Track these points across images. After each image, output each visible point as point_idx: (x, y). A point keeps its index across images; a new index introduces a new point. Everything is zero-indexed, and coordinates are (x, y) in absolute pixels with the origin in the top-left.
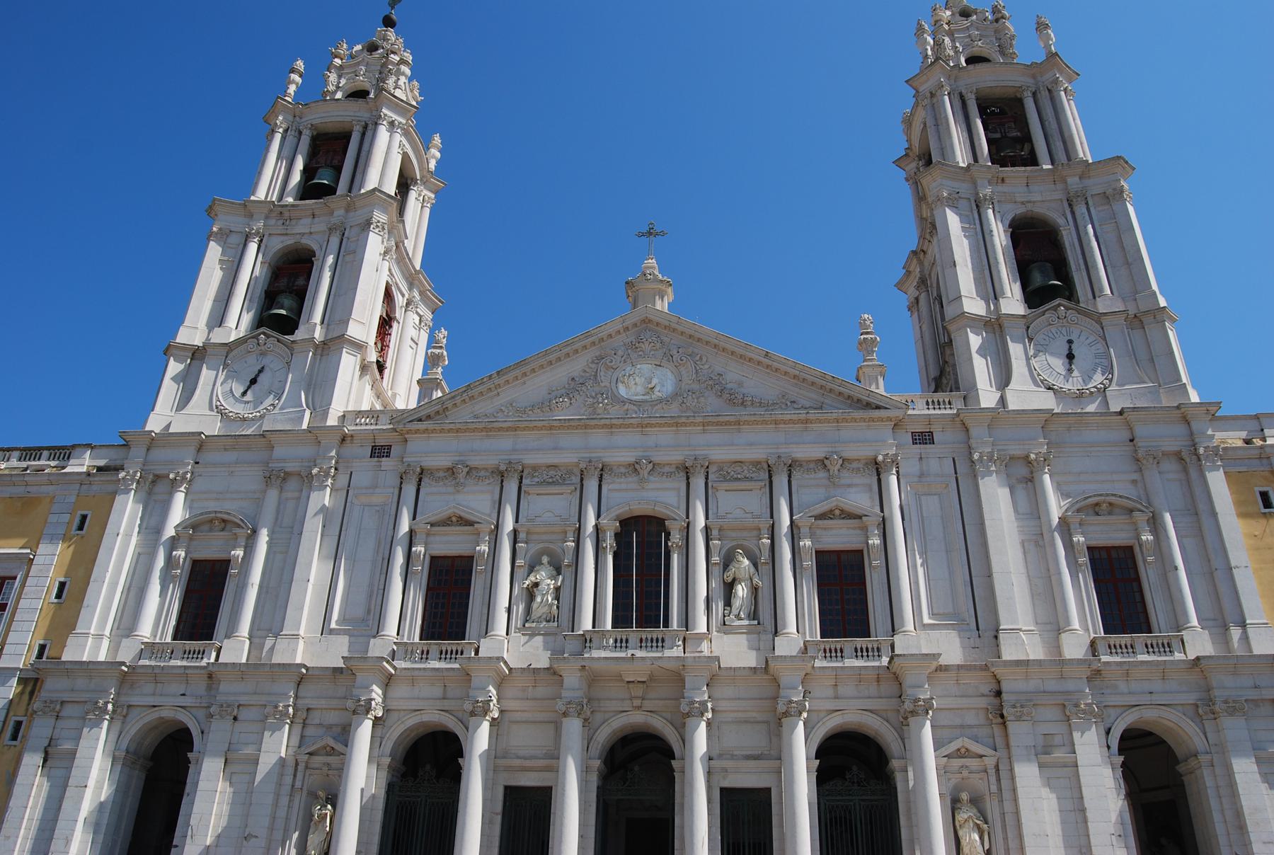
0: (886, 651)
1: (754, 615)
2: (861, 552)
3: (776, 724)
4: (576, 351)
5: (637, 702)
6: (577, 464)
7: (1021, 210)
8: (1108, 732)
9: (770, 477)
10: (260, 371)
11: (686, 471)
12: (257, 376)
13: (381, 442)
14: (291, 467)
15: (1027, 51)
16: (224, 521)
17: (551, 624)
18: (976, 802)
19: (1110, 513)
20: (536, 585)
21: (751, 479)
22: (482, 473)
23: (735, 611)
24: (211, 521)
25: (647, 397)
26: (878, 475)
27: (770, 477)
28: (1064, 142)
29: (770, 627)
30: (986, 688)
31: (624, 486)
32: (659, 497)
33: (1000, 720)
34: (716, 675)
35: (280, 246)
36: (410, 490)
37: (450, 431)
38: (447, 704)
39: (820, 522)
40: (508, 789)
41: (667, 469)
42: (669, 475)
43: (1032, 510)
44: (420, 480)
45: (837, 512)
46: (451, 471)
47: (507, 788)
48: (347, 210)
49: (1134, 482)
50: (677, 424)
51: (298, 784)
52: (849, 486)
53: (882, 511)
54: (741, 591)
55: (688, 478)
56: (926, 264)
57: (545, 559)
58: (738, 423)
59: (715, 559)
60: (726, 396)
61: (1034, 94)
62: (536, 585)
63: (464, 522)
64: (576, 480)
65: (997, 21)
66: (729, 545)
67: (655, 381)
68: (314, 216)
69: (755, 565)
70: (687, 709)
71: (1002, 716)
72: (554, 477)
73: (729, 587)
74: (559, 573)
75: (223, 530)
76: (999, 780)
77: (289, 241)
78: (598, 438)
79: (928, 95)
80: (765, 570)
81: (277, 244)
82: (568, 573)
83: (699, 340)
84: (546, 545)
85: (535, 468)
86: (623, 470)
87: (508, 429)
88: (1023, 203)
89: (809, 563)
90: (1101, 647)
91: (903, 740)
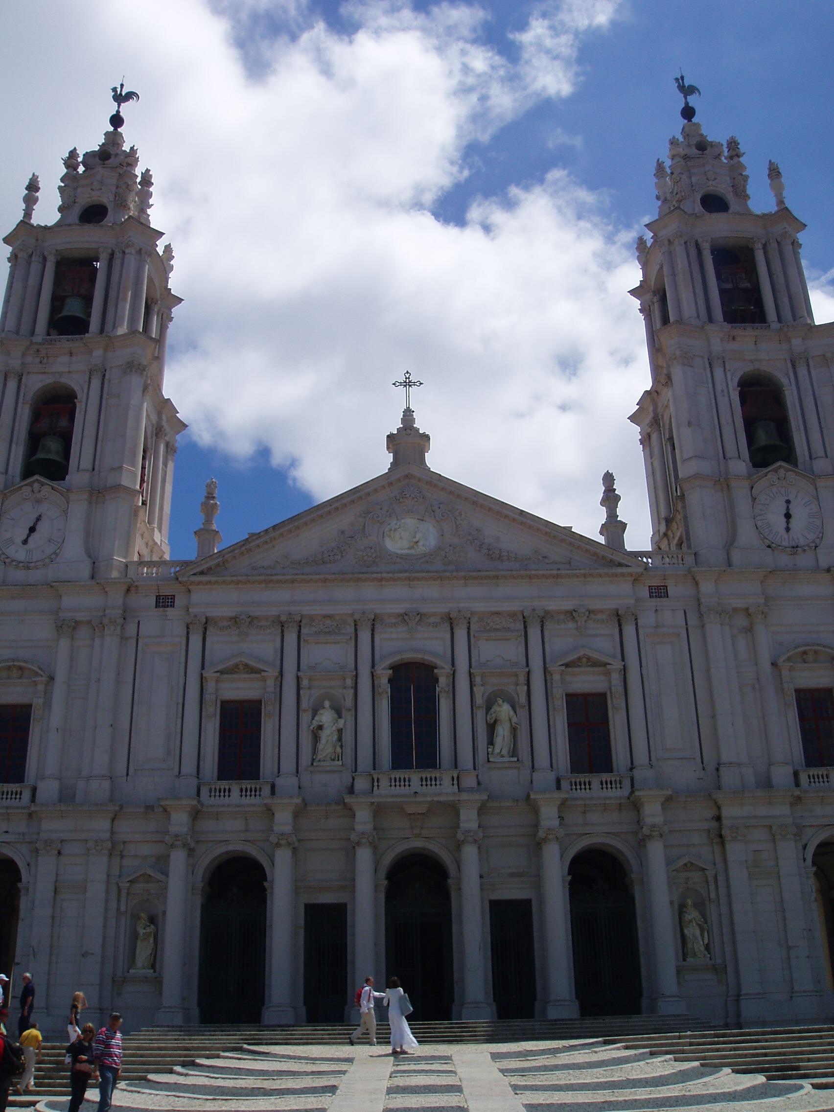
0: (627, 783)
1: (514, 752)
2: (604, 695)
3: (537, 846)
4: (345, 505)
5: (416, 831)
6: (352, 615)
7: (749, 368)
8: (805, 847)
9: (525, 627)
10: (39, 519)
11: (450, 621)
12: (36, 524)
14: (81, 616)
15: (761, 200)
17: (337, 763)
18: (700, 905)
19: (815, 661)
20: (320, 727)
21: (508, 629)
22: (263, 623)
23: (497, 750)
24: (9, 668)
25: (413, 552)
26: (620, 625)
27: (525, 627)
28: (790, 298)
29: (528, 763)
30: (710, 813)
32: (430, 644)
33: (718, 840)
35: (39, 385)
36: (196, 640)
37: (231, 582)
39: (569, 669)
41: (432, 620)
42: (435, 625)
44: (206, 629)
46: (235, 620)
48: (106, 350)
50: (441, 578)
51: (123, 908)
52: (595, 636)
55: (452, 629)
56: (660, 405)
57: (327, 704)
58: (497, 577)
60: (484, 551)
61: (765, 247)
64: (351, 629)
65: (731, 158)
67: (419, 536)
68: (71, 354)
69: (513, 707)
70: (462, 838)
71: (721, 836)
73: (492, 727)
75: (20, 678)
76: (717, 888)
77: (49, 380)
78: (369, 591)
79: (666, 242)
80: (523, 713)
81: (36, 383)
82: (348, 717)
83: (458, 496)
85: (312, 619)
86: (393, 620)
87: (286, 581)
88: (751, 361)
89: (560, 703)
90: (803, 778)
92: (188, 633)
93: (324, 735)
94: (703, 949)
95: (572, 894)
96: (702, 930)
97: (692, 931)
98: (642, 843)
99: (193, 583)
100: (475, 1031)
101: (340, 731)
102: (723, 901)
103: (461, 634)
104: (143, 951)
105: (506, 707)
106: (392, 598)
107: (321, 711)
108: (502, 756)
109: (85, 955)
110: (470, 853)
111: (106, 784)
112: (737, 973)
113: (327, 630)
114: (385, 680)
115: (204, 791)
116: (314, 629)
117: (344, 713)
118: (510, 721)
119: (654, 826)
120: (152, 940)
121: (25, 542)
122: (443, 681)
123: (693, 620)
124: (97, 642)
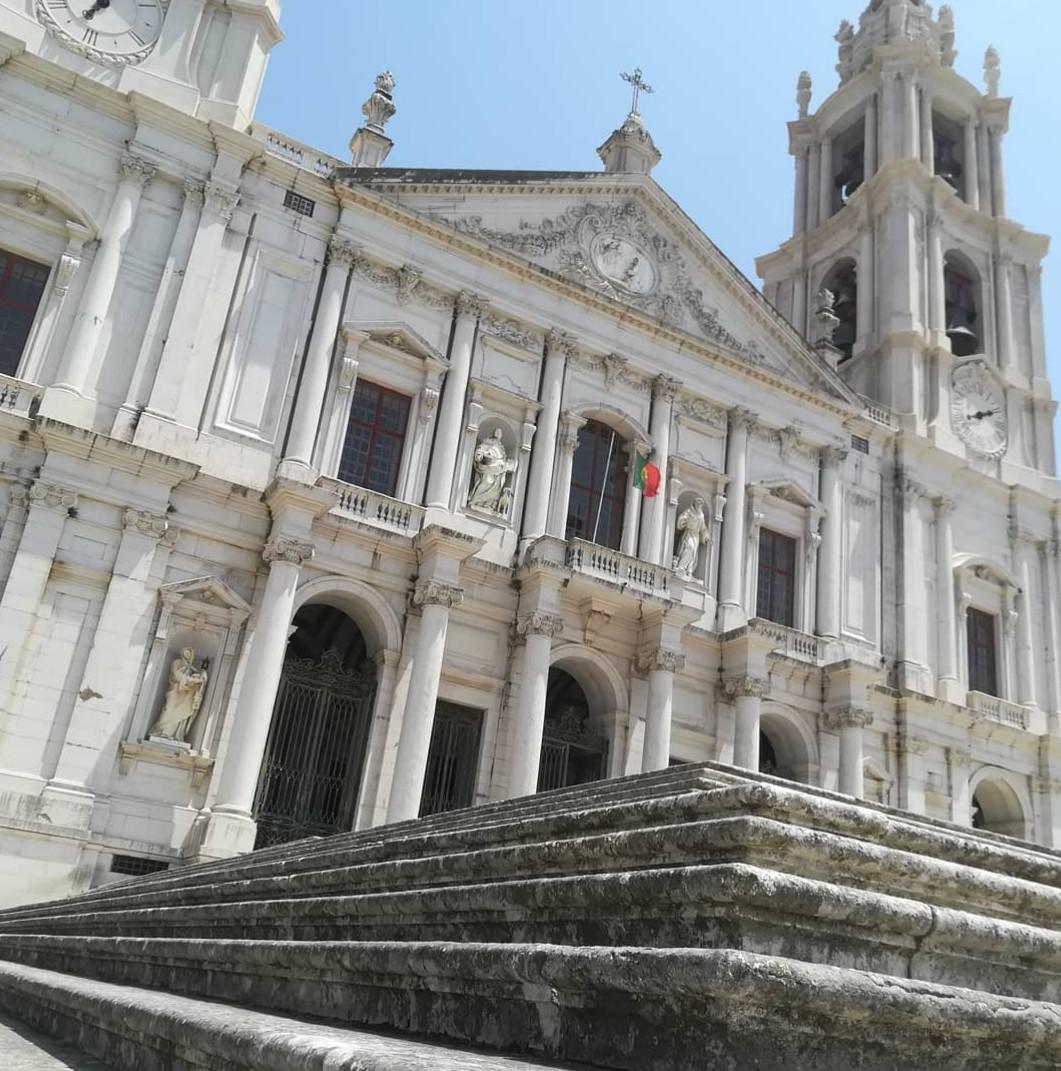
13: (303, 190)
14: (167, 167)
16: (45, 201)
20: (485, 461)
22: (431, 294)
31: (588, 379)
32: (626, 406)
38: (377, 578)
41: (632, 378)
42: (636, 386)
43: (936, 554)
45: (786, 492)
49: (1005, 557)
54: (692, 542)
62: (485, 461)
63: (406, 347)
72: (513, 334)
84: (502, 417)
91: (818, 745)
92: (327, 261)
101: (509, 475)
106: (597, 332)
109: (88, 694)
114: (573, 431)
118: (701, 534)
120: (198, 698)
121: (89, 15)
124: (188, 215)
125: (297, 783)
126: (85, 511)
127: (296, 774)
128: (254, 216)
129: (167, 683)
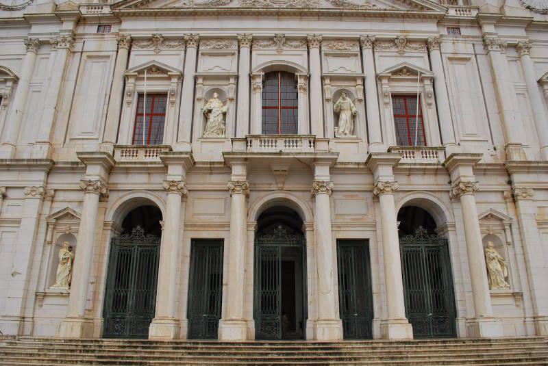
13: (103, 22)
18: (498, 247)
20: (210, 111)
23: (341, 130)
32: (293, 57)
34: (335, 168)
36: (123, 53)
40: (195, 242)
47: (193, 240)
53: (431, 69)
54: (345, 116)
57: (216, 95)
59: (329, 95)
62: (210, 111)
66: (335, 89)
69: (354, 102)
71: (513, 196)
73: (337, 116)
74: (224, 103)
93: (212, 117)
94: (503, 280)
95: (400, 237)
96: (502, 265)
97: (495, 266)
98: (456, 198)
99: (123, 14)
100: (340, 354)
102: (517, 243)
103: (315, 51)
104: (62, 270)
105: (348, 100)
107: (211, 100)
108: (346, 134)
110: (323, 200)
111: (46, 147)
112: (532, 299)
113: (218, 47)
114: (259, 81)
115: (118, 153)
116: (209, 47)
117: (228, 102)
119: (468, 183)
120: (69, 264)
122: (301, 81)
123: (480, 49)
125: (127, 296)
126: (11, 194)
127: (126, 291)
128: (84, 42)
129: (56, 261)
